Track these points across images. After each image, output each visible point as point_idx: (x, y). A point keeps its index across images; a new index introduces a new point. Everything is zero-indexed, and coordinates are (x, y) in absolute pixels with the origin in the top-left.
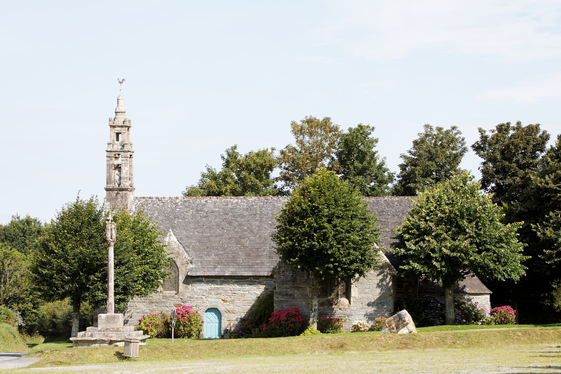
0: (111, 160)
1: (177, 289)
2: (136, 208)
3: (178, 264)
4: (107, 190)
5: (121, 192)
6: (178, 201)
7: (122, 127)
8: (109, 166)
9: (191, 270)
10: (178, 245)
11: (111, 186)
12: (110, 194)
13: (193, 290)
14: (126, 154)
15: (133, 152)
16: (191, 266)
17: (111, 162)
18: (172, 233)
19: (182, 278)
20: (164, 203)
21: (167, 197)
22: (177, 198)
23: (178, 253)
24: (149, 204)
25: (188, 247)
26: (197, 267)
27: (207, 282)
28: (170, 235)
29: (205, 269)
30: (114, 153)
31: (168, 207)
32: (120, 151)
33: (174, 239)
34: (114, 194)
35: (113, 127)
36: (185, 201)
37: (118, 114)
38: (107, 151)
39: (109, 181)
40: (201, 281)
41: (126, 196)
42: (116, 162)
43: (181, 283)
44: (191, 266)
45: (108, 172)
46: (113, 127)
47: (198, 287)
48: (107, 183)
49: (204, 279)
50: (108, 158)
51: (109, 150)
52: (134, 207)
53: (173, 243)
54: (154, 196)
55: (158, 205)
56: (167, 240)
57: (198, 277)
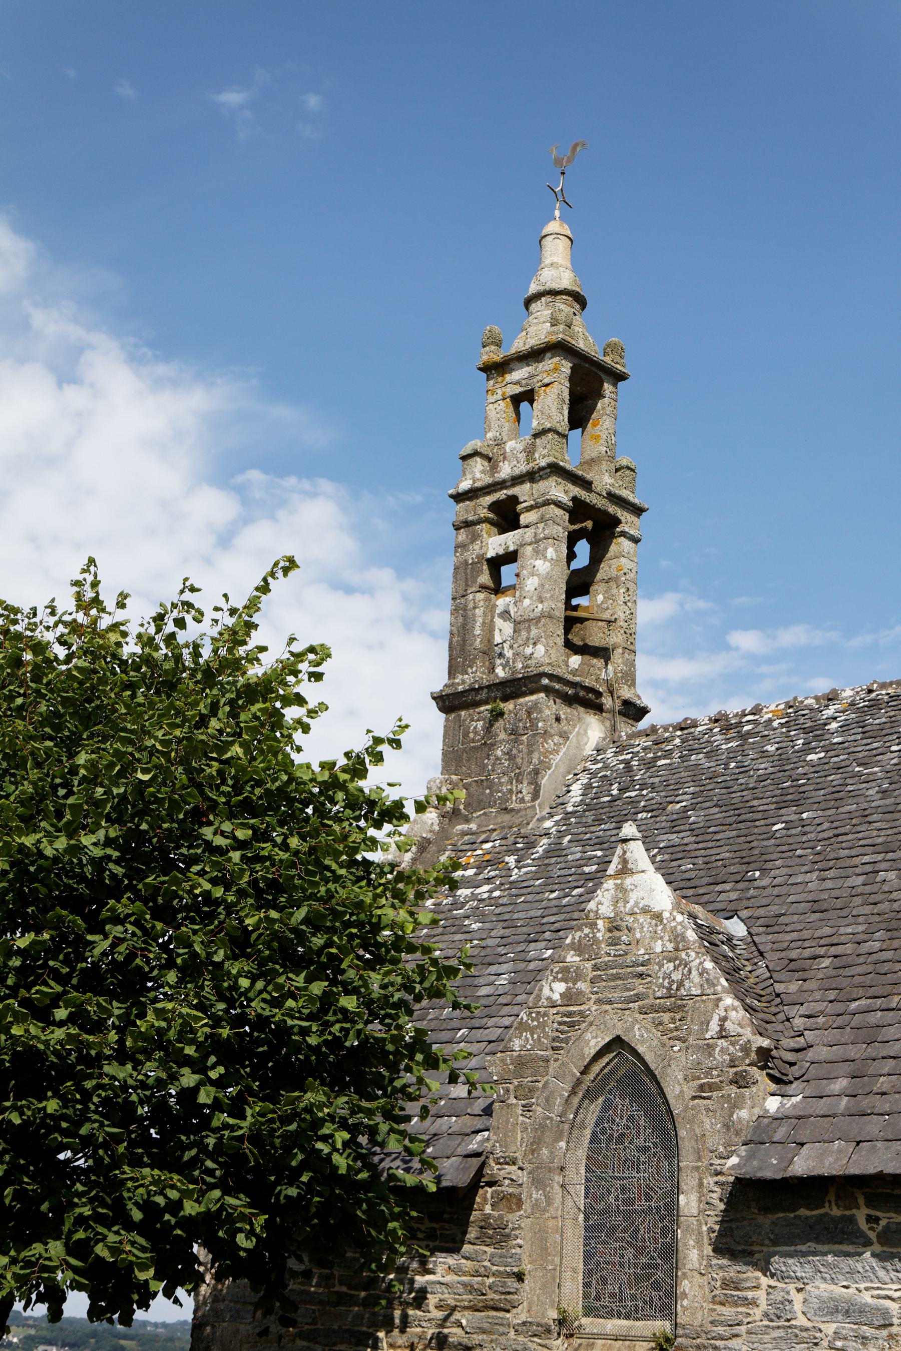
0: (475, 538)
1: (666, 1303)
2: (588, 787)
3: (677, 1088)
4: (449, 702)
5: (509, 706)
6: (830, 712)
7: (534, 355)
8: (464, 573)
9: (759, 1137)
10: (678, 938)
11: (464, 681)
12: (459, 722)
13: (779, 1312)
14: (542, 486)
15: (638, 511)
16: (773, 1104)
17: (471, 555)
18: (637, 852)
19: (698, 1205)
20: (744, 737)
21: (773, 706)
22: (831, 697)
23: (676, 1003)
24: (668, 754)
25: (797, 968)
26: (822, 1106)
27: (886, 1238)
28: (625, 870)
29: (873, 1126)
30: (488, 500)
31: (764, 754)
32: (517, 480)
33: (652, 889)
34: (475, 722)
35: (496, 369)
36: (875, 705)
37: (534, 307)
38: (459, 497)
39: (459, 656)
40: (840, 1236)
41: (534, 727)
42: (495, 544)
43: (695, 1252)
44: (773, 1104)
45: (455, 611)
46: (496, 369)
47: (822, 1289)
48: (452, 673)
49: (861, 1215)
50: (463, 536)
51: (465, 485)
52: (576, 789)
53: (643, 926)
54: (702, 715)
55: (708, 755)
56: (606, 910)
57: (814, 1187)
